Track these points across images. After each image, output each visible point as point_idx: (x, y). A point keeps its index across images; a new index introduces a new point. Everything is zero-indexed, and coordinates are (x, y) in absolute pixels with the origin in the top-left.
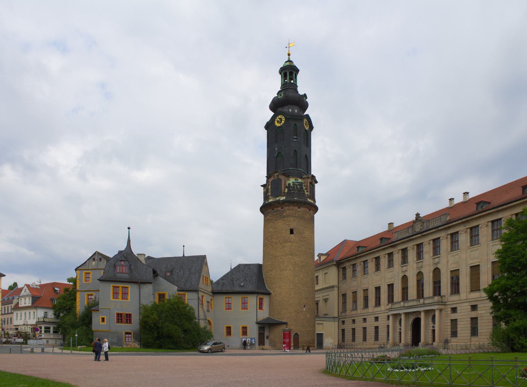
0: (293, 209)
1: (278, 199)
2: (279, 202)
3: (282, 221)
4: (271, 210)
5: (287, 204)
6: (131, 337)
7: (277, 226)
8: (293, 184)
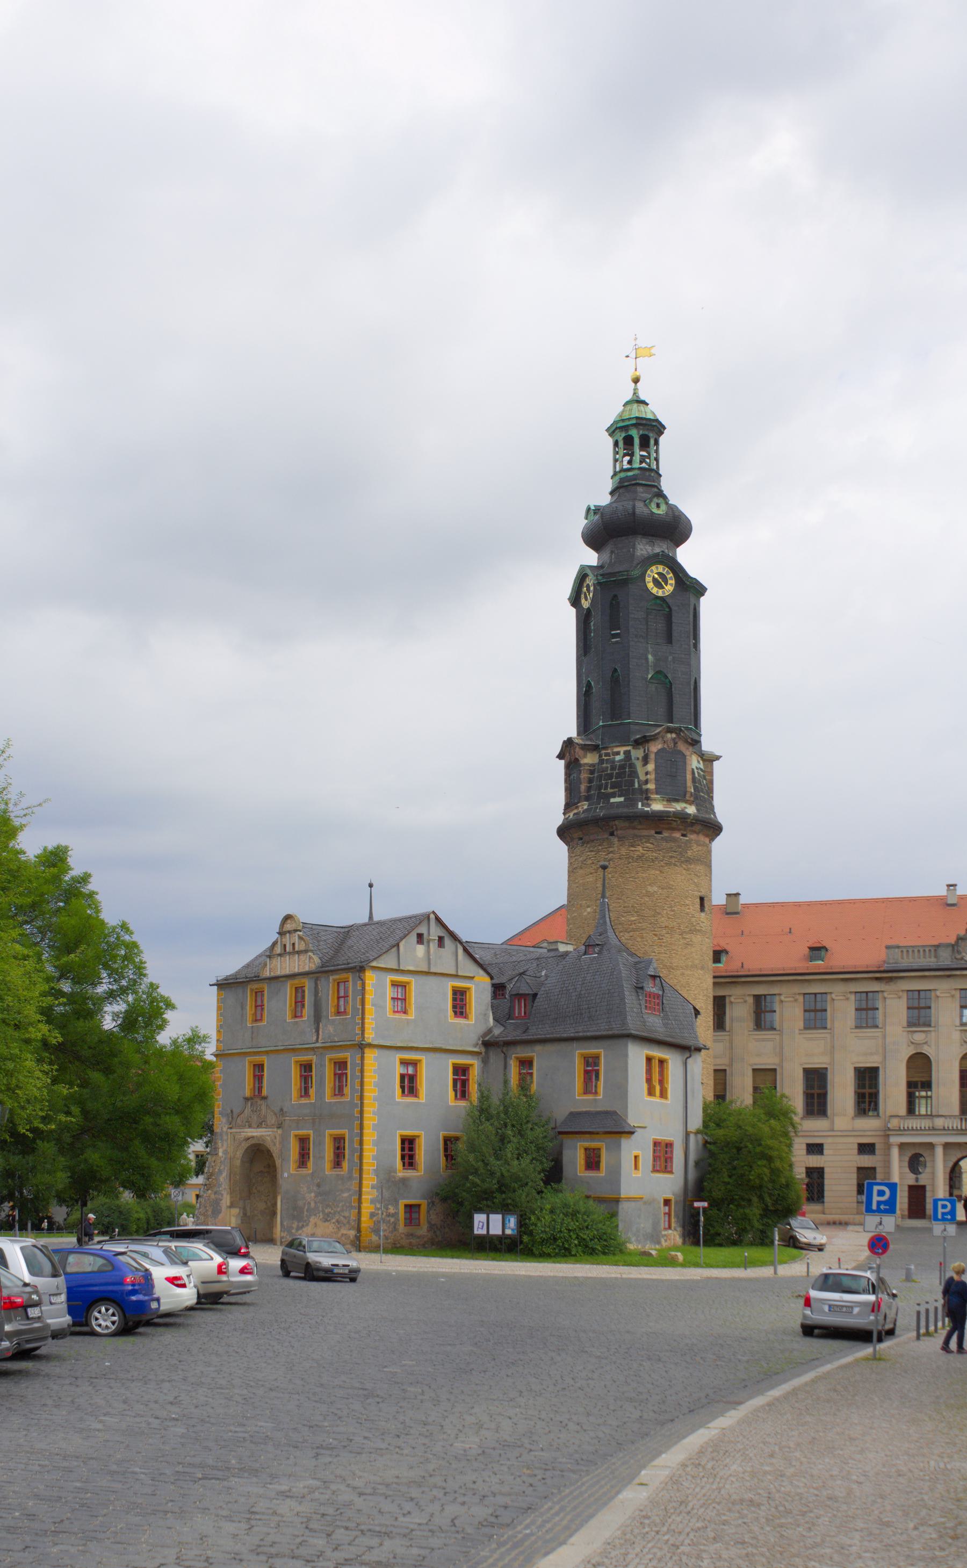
0: (704, 845)
1: (678, 806)
2: (685, 818)
3: (684, 871)
4: (653, 832)
5: (697, 828)
6: (669, 1214)
7: (672, 883)
8: (698, 773)
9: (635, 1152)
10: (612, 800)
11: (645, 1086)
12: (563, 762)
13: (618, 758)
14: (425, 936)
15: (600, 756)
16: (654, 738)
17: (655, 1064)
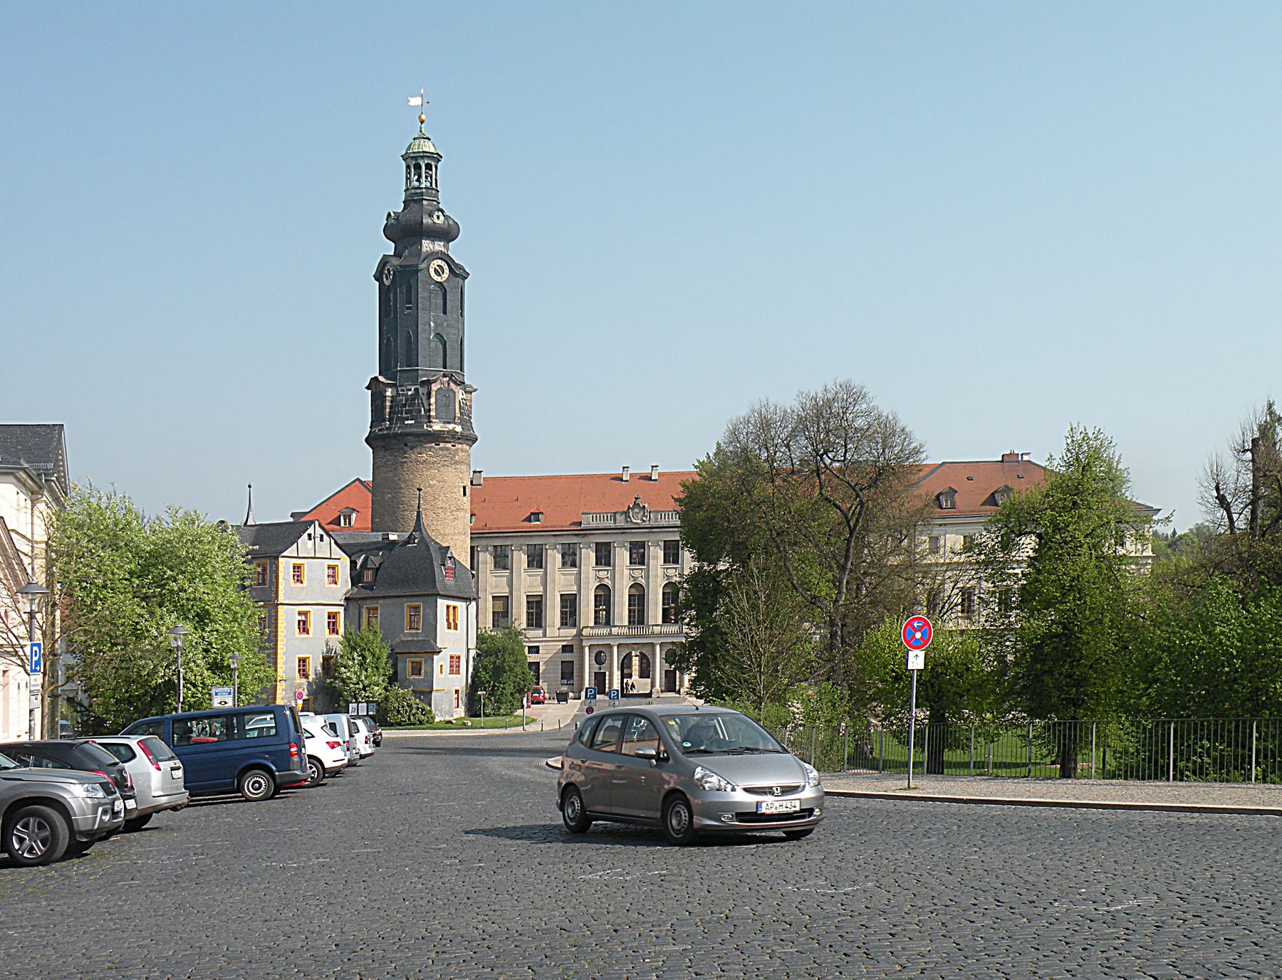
1: (451, 426)
9: (441, 664)
10: (406, 422)
11: (446, 623)
12: (370, 391)
13: (410, 393)
14: (313, 535)
15: (397, 391)
16: (435, 381)
17: (451, 609)
